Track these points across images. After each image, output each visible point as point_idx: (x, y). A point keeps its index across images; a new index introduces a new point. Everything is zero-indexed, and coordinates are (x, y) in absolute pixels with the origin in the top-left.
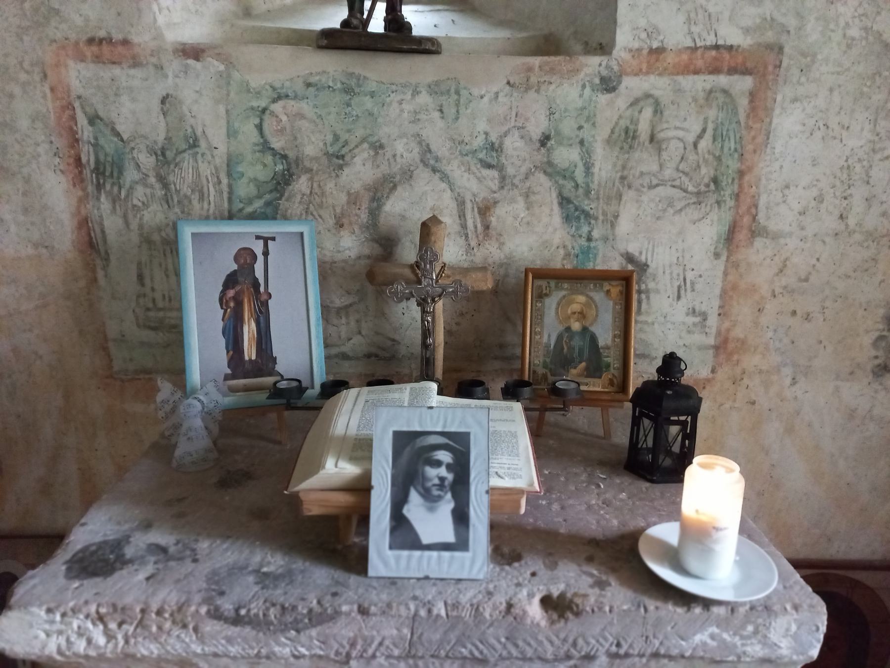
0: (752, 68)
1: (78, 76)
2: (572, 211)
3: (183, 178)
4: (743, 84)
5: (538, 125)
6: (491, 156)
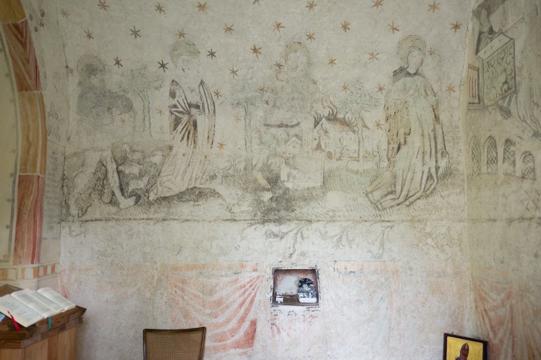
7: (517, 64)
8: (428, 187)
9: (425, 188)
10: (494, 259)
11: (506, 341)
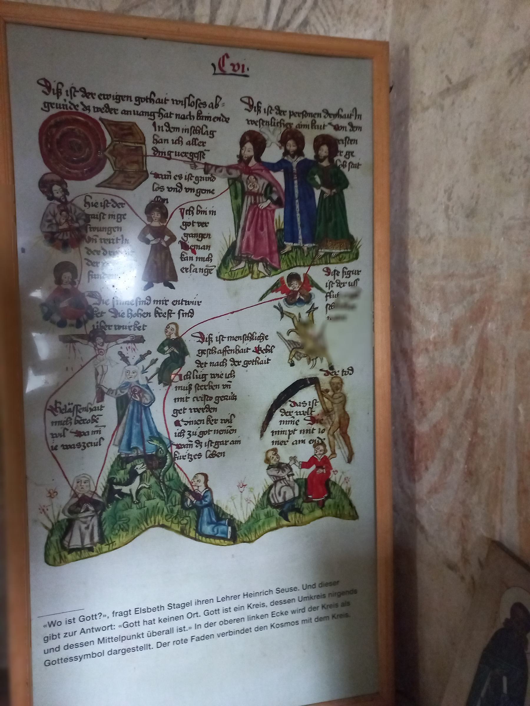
8: (286, 16)
9: (278, 18)
10: (447, 208)
11: (450, 431)
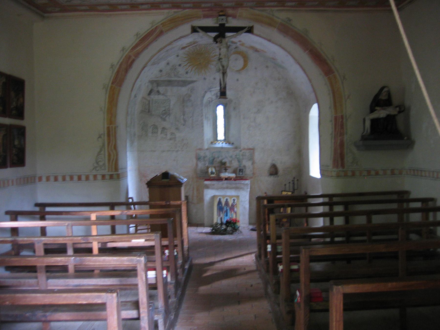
0: (252, 150)
1: (198, 151)
2: (239, 161)
3: (206, 159)
4: (252, 151)
5: (235, 154)
6: (231, 157)
7: (171, 107)
